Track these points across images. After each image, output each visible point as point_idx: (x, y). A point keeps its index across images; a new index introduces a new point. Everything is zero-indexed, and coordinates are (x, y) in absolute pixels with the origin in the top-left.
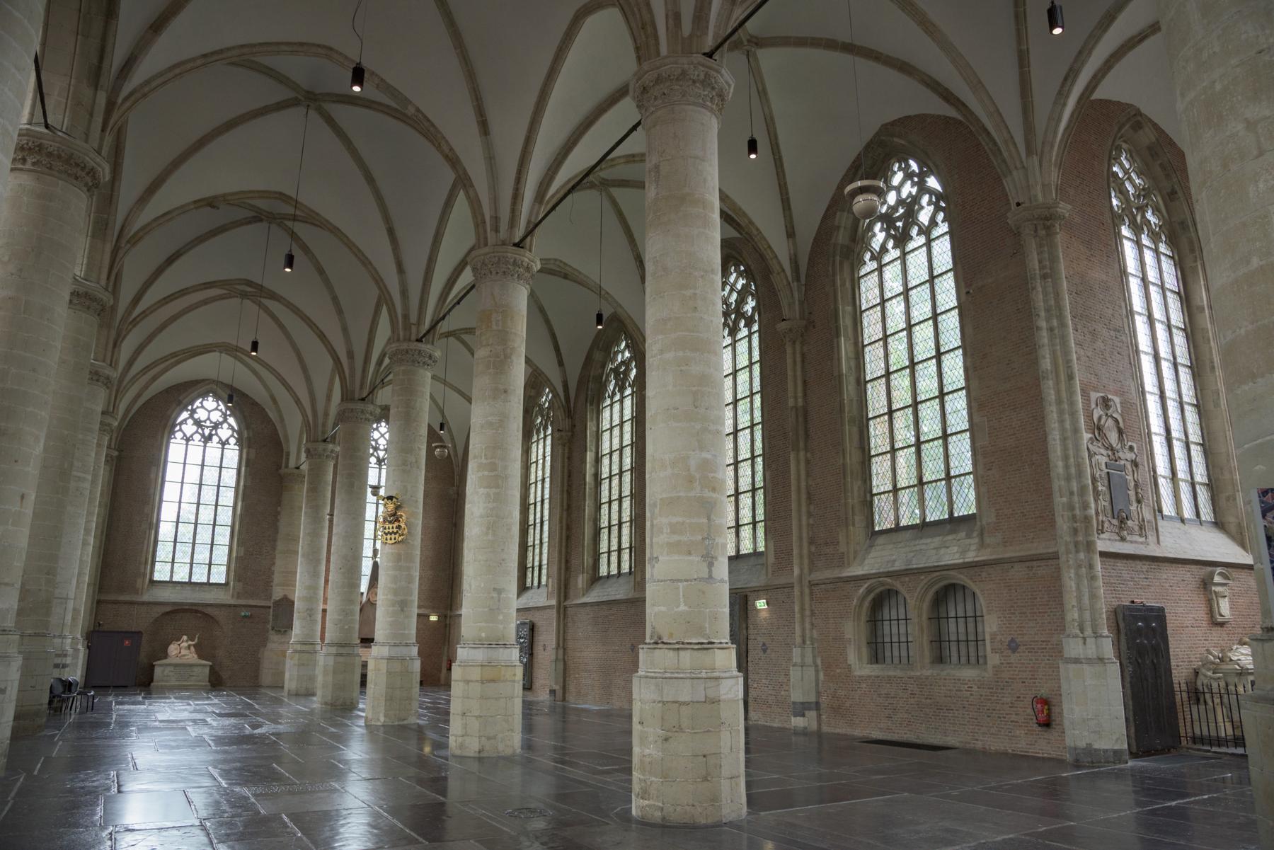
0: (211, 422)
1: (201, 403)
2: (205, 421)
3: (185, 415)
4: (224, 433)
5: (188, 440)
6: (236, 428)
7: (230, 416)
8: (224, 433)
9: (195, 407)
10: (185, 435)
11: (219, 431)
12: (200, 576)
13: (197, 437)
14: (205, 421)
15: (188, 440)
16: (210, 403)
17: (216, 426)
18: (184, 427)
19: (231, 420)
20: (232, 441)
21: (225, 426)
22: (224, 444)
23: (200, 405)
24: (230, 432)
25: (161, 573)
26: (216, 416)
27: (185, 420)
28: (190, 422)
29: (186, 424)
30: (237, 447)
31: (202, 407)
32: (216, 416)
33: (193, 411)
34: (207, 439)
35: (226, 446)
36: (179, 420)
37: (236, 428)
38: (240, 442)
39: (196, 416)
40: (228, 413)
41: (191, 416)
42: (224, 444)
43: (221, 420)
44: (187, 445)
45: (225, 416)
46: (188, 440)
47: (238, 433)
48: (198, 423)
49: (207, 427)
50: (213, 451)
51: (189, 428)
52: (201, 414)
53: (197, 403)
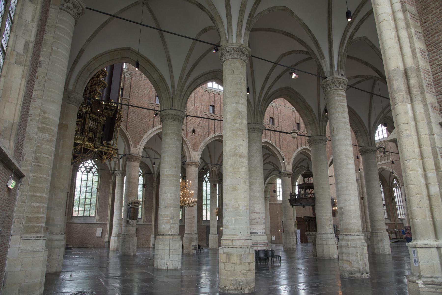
0: (89, 167)
2: (88, 167)
3: (82, 165)
4: (93, 170)
5: (82, 173)
6: (97, 168)
7: (95, 165)
13: (85, 171)
14: (88, 167)
15: (82, 172)
17: (91, 168)
18: (81, 169)
20: (96, 172)
21: (94, 168)
22: (93, 173)
24: (95, 170)
27: (82, 166)
28: (83, 167)
29: (82, 168)
30: (98, 175)
32: (91, 165)
35: (94, 174)
36: (80, 166)
37: (97, 168)
39: (85, 165)
40: (95, 164)
41: (83, 165)
43: (92, 166)
44: (93, 175)
46: (82, 172)
47: (98, 170)
48: (86, 167)
49: (88, 169)
51: (83, 169)
52: (87, 165)
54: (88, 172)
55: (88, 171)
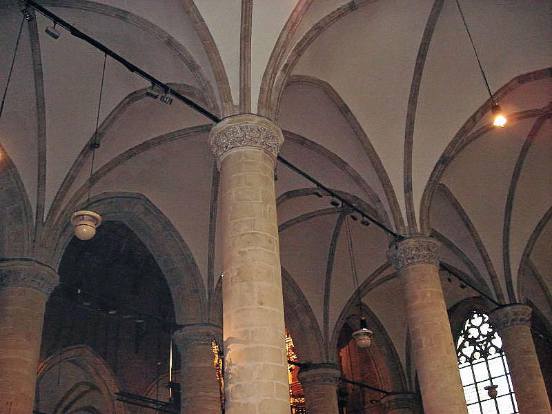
0: (484, 336)
1: (470, 323)
2: (478, 338)
9: (466, 329)
10: (465, 356)
11: (464, 350)
13: (477, 355)
14: (478, 338)
15: (470, 360)
16: (477, 320)
17: (490, 337)
18: (464, 350)
23: (470, 325)
26: (486, 329)
27: (464, 341)
28: (467, 343)
31: (473, 326)
33: (467, 333)
34: (485, 354)
39: (470, 337)
41: (466, 339)
46: (470, 360)
48: (473, 342)
49: (482, 342)
52: (474, 333)
53: (467, 325)
54: (485, 354)
55: (483, 348)
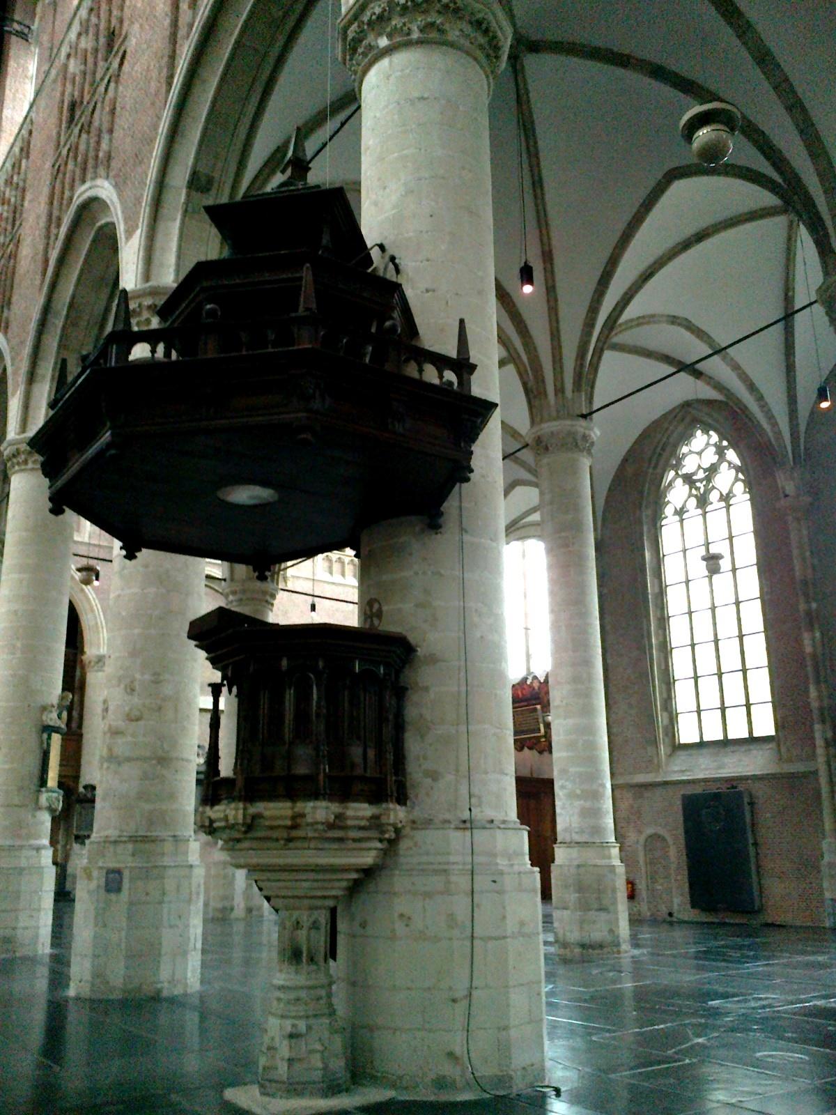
8: (726, 479)
12: (738, 730)
17: (712, 470)
19: (731, 455)
20: (739, 487)
25: (687, 733)
26: (710, 457)
32: (710, 457)
34: (703, 502)
38: (750, 485)
40: (725, 443)
42: (726, 498)
43: (715, 459)
45: (720, 452)
48: (689, 479)
50: (717, 516)
54: (703, 502)
